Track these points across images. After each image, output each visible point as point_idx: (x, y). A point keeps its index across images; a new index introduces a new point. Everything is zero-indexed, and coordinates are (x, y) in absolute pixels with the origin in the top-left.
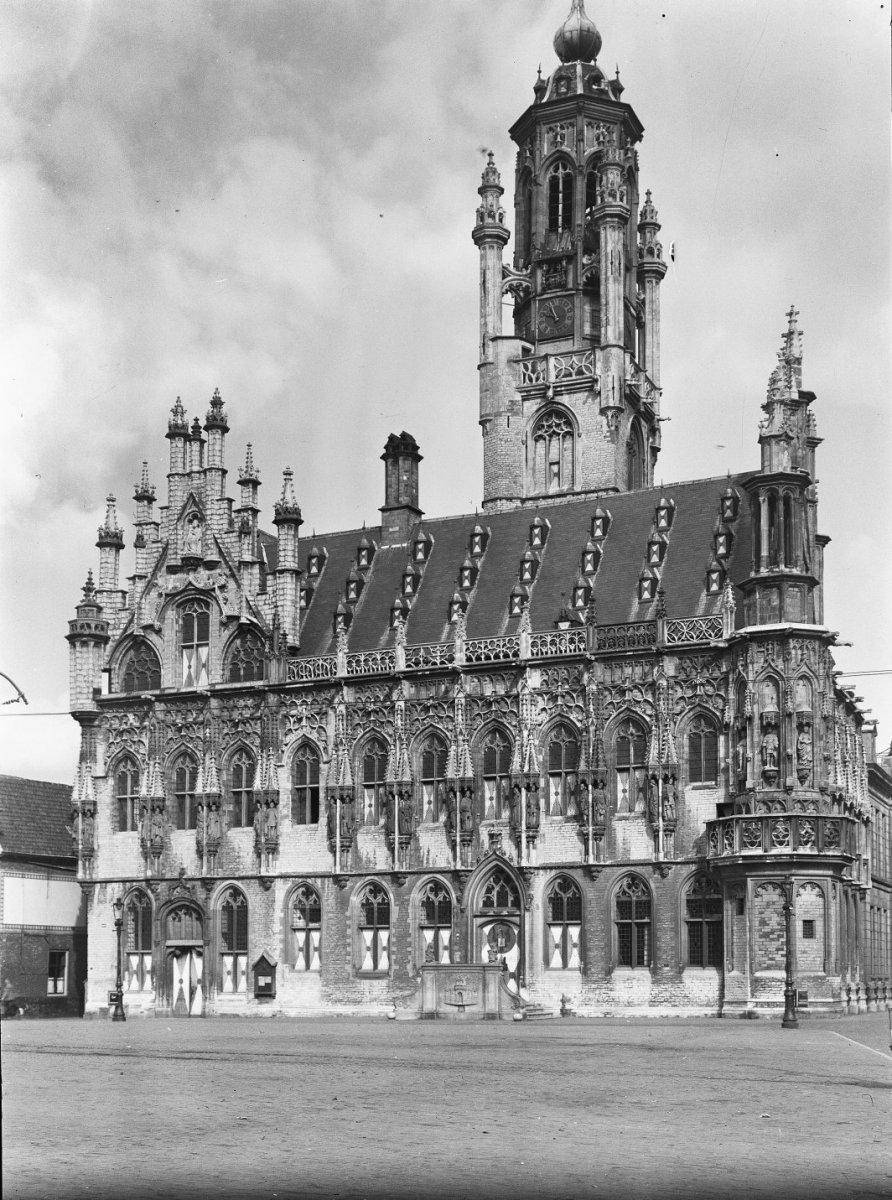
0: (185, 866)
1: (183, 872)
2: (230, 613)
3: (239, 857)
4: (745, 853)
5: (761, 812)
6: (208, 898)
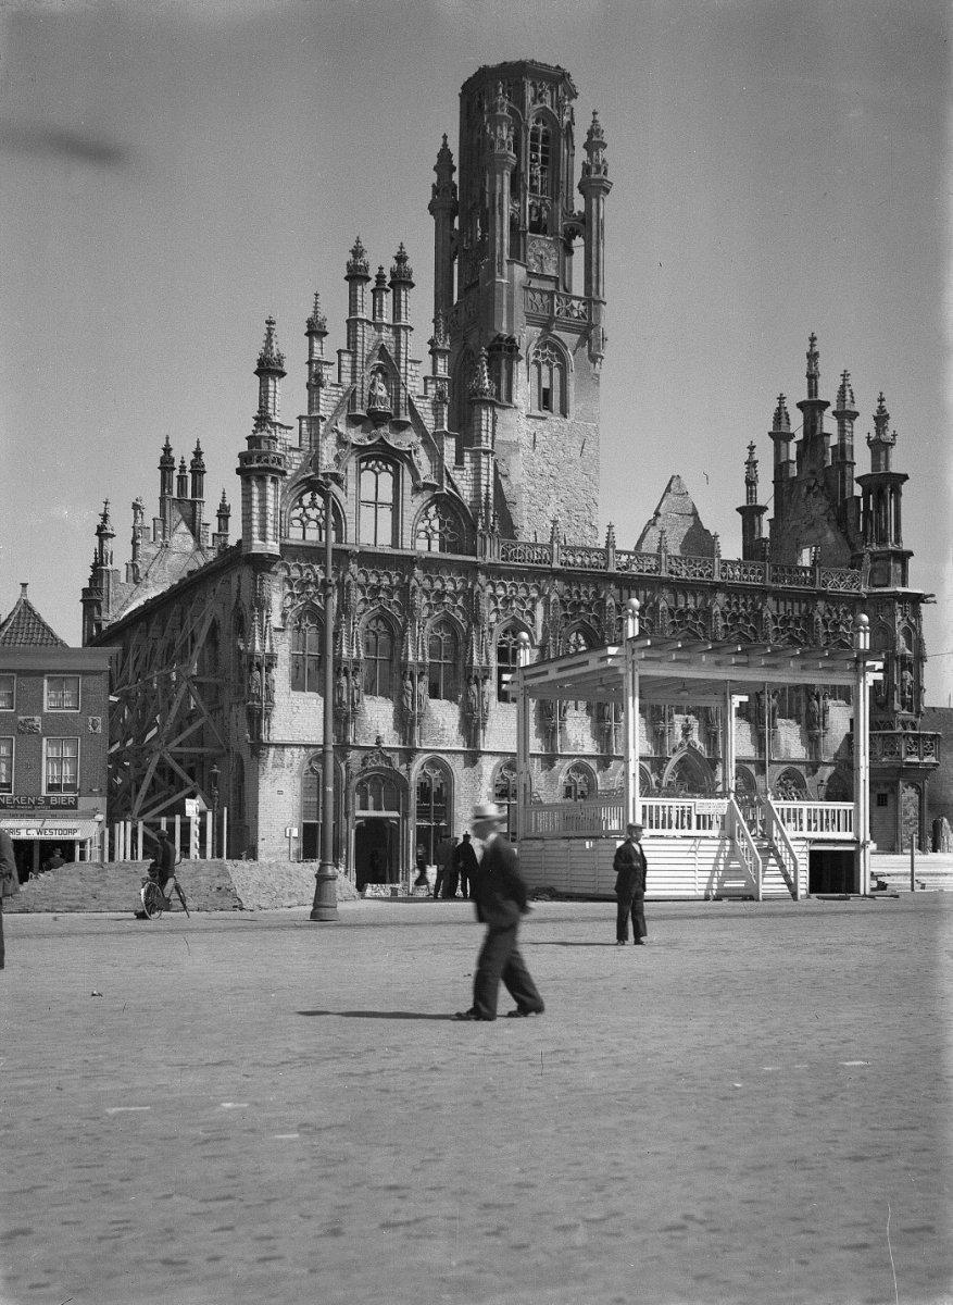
0: (381, 734)
1: (379, 740)
2: (427, 481)
3: (443, 729)
4: (909, 760)
5: (899, 729)
6: (408, 770)
